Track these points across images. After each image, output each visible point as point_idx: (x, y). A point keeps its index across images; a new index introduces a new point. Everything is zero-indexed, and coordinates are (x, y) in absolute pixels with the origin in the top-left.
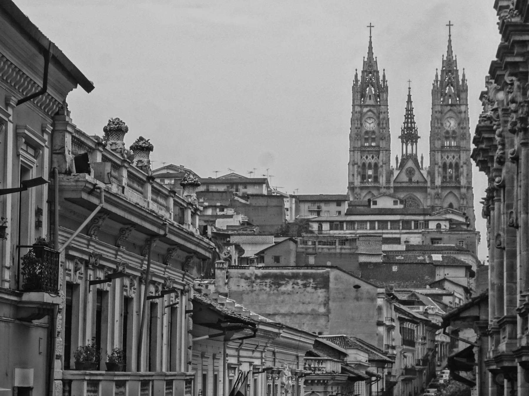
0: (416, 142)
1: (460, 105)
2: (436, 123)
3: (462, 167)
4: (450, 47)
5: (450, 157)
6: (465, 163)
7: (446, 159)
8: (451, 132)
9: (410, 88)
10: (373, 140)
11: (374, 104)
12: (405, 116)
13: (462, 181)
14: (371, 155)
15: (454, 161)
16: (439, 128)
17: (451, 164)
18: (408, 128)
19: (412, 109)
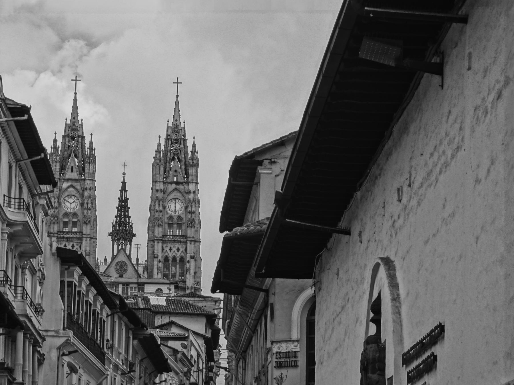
0: (131, 241)
1: (188, 183)
2: (157, 205)
3: (188, 262)
4: (177, 110)
5: (174, 249)
6: (192, 257)
7: (168, 251)
8: (175, 218)
9: (124, 174)
10: (75, 224)
11: (77, 178)
12: (117, 208)
13: (188, 281)
14: (72, 243)
15: (178, 255)
16: (161, 211)
17: (174, 259)
18: (119, 223)
19: (126, 200)
